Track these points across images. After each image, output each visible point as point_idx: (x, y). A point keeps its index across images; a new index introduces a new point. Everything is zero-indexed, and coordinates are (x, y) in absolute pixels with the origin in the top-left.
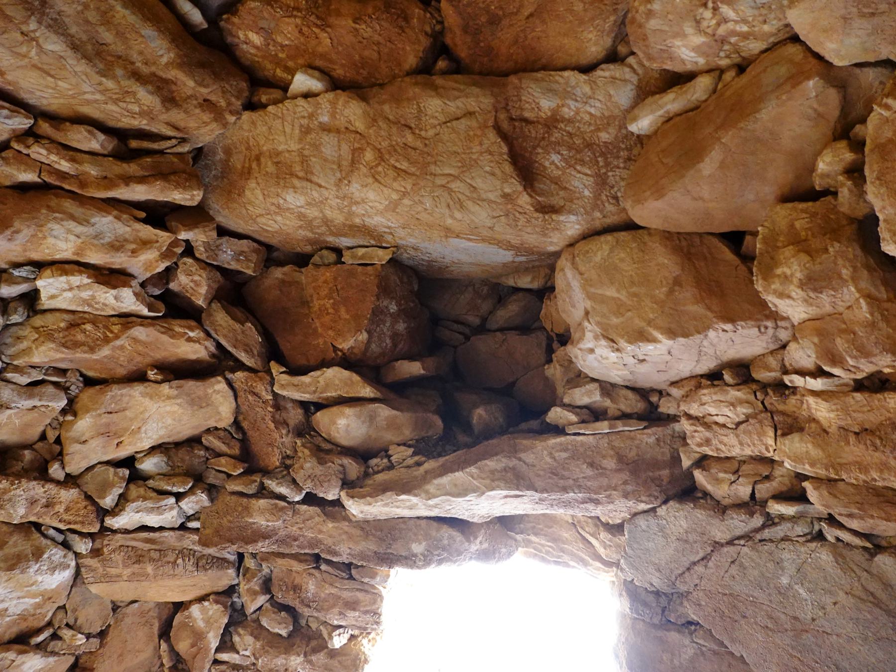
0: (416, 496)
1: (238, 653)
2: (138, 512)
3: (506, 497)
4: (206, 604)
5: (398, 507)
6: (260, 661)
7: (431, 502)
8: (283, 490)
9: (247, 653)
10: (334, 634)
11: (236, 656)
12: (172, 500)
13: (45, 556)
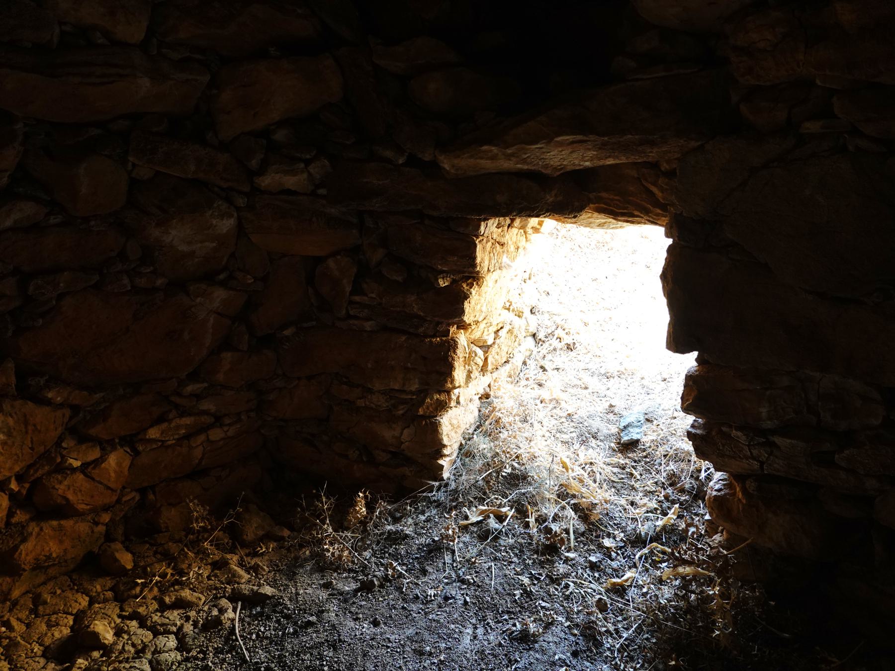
0: (495, 145)
1: (367, 296)
2: (277, 173)
3: (573, 142)
4: (339, 257)
5: (482, 158)
6: (384, 299)
7: (509, 151)
8: (388, 154)
9: (373, 295)
10: (442, 276)
11: (366, 298)
12: (302, 165)
13: (215, 205)
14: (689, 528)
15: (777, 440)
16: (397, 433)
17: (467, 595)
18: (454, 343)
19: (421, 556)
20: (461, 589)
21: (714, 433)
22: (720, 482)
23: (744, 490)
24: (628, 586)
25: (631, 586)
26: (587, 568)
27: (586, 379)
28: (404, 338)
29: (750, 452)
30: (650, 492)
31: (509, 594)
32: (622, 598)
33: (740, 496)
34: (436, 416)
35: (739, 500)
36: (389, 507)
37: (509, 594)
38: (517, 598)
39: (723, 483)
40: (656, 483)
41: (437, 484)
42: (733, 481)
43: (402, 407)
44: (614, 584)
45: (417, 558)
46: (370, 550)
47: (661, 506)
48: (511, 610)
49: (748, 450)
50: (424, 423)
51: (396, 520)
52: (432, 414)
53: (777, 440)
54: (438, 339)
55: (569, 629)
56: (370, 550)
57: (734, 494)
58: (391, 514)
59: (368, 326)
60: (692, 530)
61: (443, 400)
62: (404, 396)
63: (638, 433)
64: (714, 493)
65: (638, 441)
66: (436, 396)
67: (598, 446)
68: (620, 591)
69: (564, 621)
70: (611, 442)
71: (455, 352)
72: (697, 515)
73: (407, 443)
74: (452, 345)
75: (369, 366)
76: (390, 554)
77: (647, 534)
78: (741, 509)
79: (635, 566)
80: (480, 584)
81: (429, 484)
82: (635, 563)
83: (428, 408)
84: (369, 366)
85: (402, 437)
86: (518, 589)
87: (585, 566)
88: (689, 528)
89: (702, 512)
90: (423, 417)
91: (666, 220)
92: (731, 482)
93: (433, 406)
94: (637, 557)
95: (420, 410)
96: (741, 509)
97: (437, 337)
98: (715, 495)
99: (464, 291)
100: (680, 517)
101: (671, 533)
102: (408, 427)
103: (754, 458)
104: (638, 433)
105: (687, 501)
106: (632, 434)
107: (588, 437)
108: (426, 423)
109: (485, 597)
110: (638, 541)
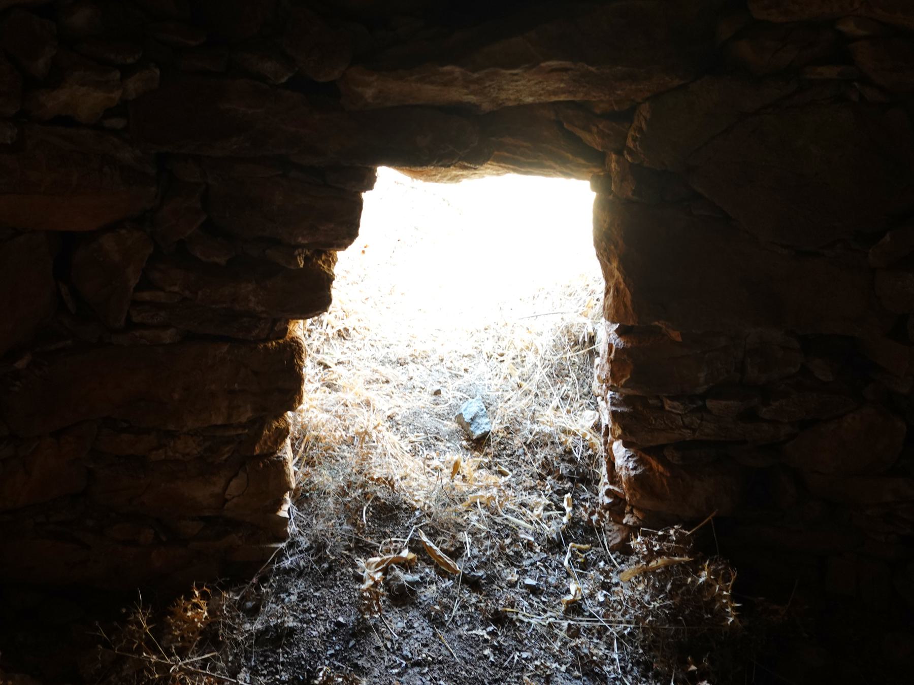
6: (200, 293)
9: (176, 289)
10: (296, 252)
14: (591, 518)
15: (709, 404)
16: (217, 490)
17: (435, 679)
18: (298, 346)
19: (336, 650)
20: (424, 674)
21: (640, 408)
22: (630, 459)
23: (663, 461)
24: (580, 600)
25: (583, 599)
26: (529, 595)
27: (388, 371)
28: (225, 348)
29: (682, 420)
30: (531, 488)
31: (480, 658)
32: (583, 616)
33: (661, 469)
34: (275, 453)
35: (661, 474)
36: (237, 598)
37: (480, 658)
38: (492, 659)
39: (634, 459)
40: (531, 476)
41: (283, 545)
42: (643, 455)
43: (227, 449)
44: (568, 603)
45: (332, 655)
46: (244, 669)
47: (552, 500)
48: (497, 677)
49: (680, 420)
50: (261, 465)
51: (253, 613)
52: (271, 451)
53: (709, 404)
54: (274, 343)
55: (569, 673)
56: (244, 669)
57: (651, 469)
58: (240, 606)
59: (168, 336)
60: (595, 517)
61: (284, 428)
62: (233, 433)
63: (486, 424)
64: (633, 473)
65: (487, 433)
66: (275, 424)
67: (448, 448)
68: (575, 608)
69: (558, 666)
70: (461, 440)
71: (301, 360)
72: (585, 500)
73: (235, 500)
74: (294, 351)
75: (176, 396)
76: (283, 664)
77: (558, 534)
78: (665, 483)
79: (568, 575)
80: (440, 658)
81: (277, 548)
82: (567, 573)
83: (265, 443)
84: (176, 396)
85: (227, 493)
86: (485, 648)
87: (527, 593)
88: (591, 518)
89: (587, 496)
90: (261, 457)
91: (591, 175)
92: (641, 457)
93: (272, 439)
94: (566, 563)
95: (256, 448)
96: (665, 483)
97: (271, 340)
98: (635, 475)
99: (326, 272)
100: (575, 507)
101: (574, 528)
102: (236, 475)
103: (686, 427)
104: (486, 424)
105: (572, 488)
106: (483, 426)
107: (433, 440)
108: (265, 466)
109: (457, 673)
110: (555, 546)
